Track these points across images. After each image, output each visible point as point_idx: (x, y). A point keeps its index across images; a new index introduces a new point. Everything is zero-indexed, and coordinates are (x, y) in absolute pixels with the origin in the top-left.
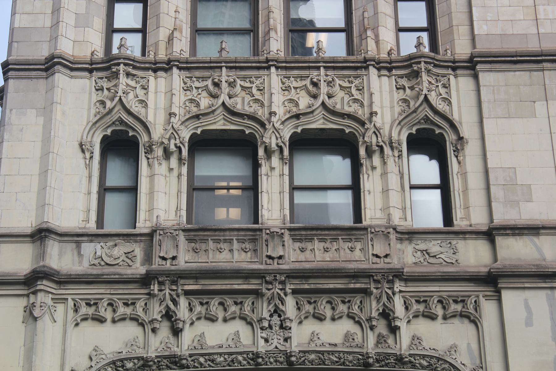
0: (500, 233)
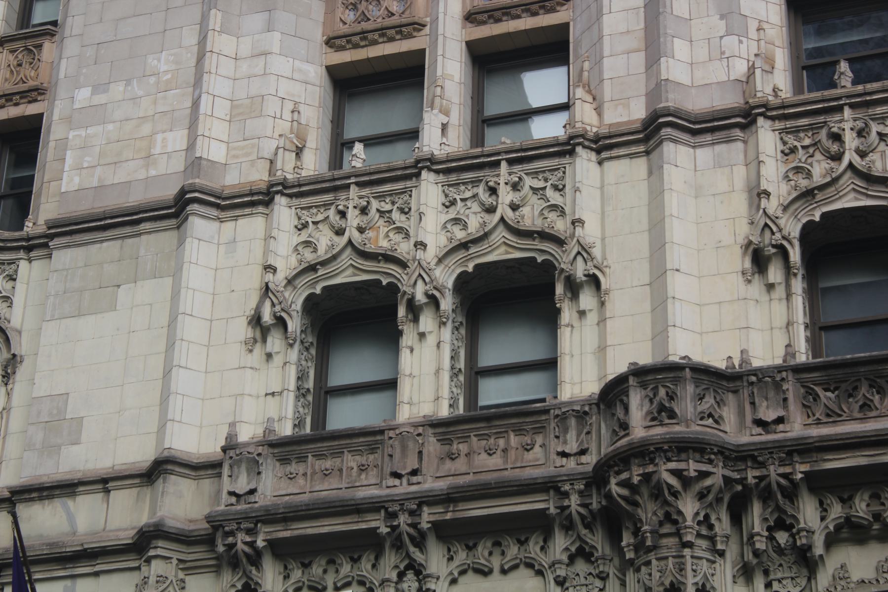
0: (22, 498)
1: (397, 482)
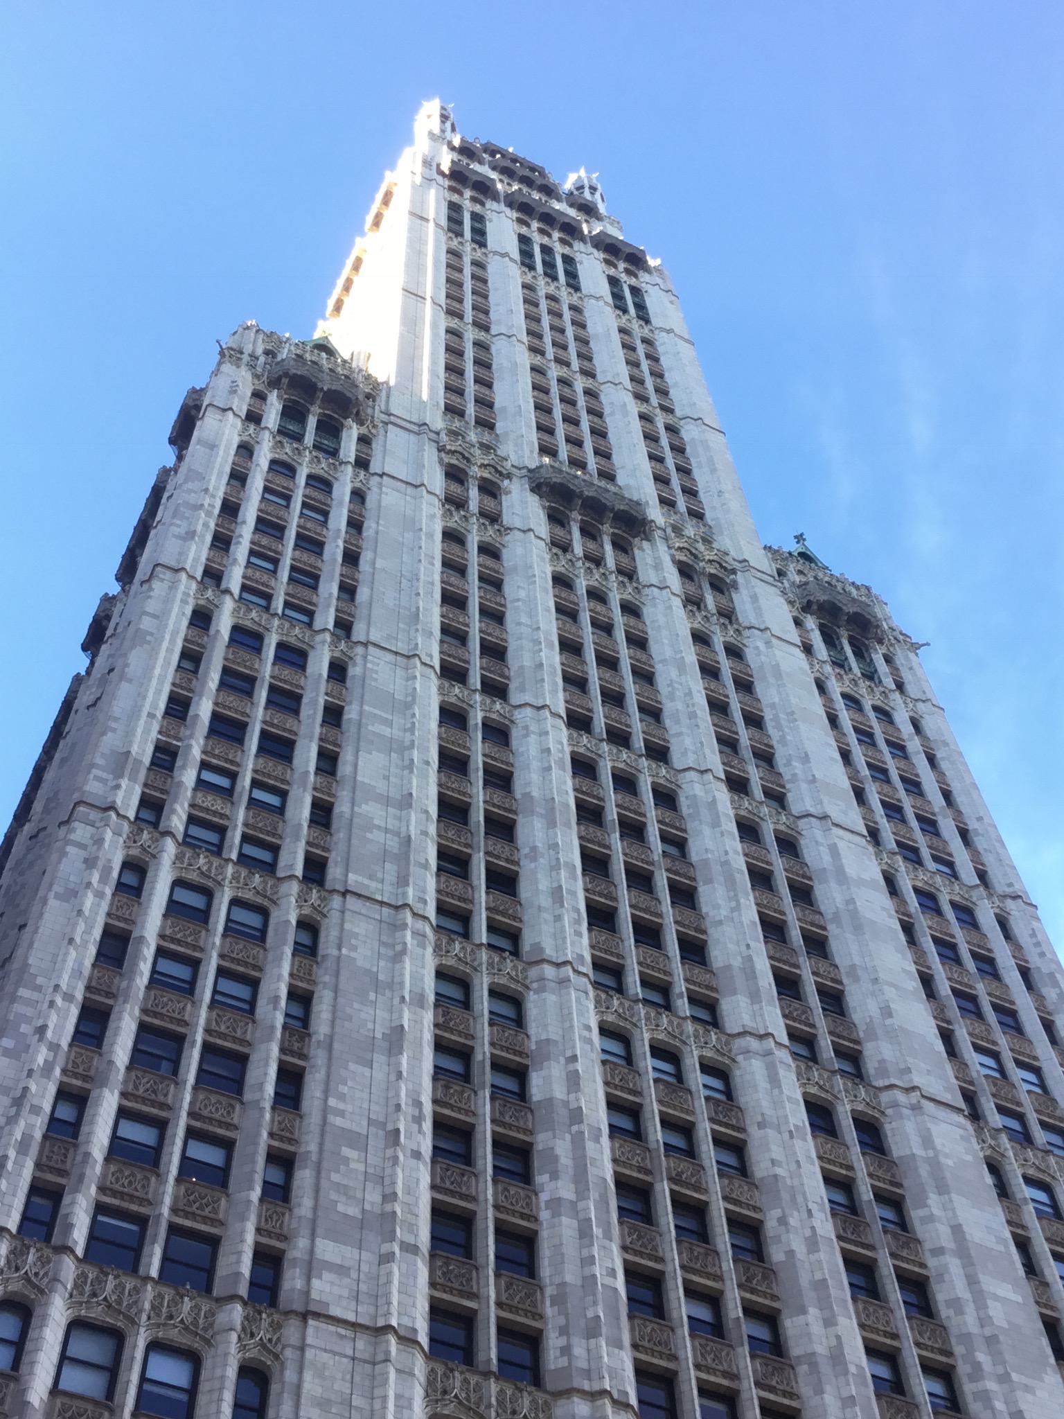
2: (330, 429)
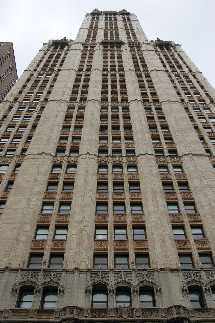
1: (30, 318)
2: (63, 48)
